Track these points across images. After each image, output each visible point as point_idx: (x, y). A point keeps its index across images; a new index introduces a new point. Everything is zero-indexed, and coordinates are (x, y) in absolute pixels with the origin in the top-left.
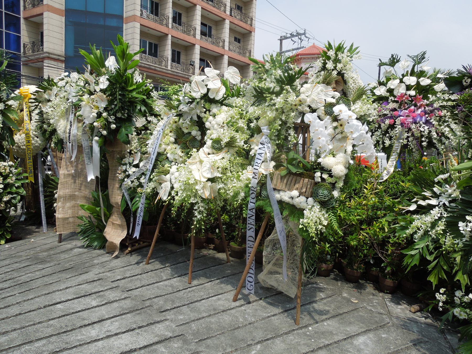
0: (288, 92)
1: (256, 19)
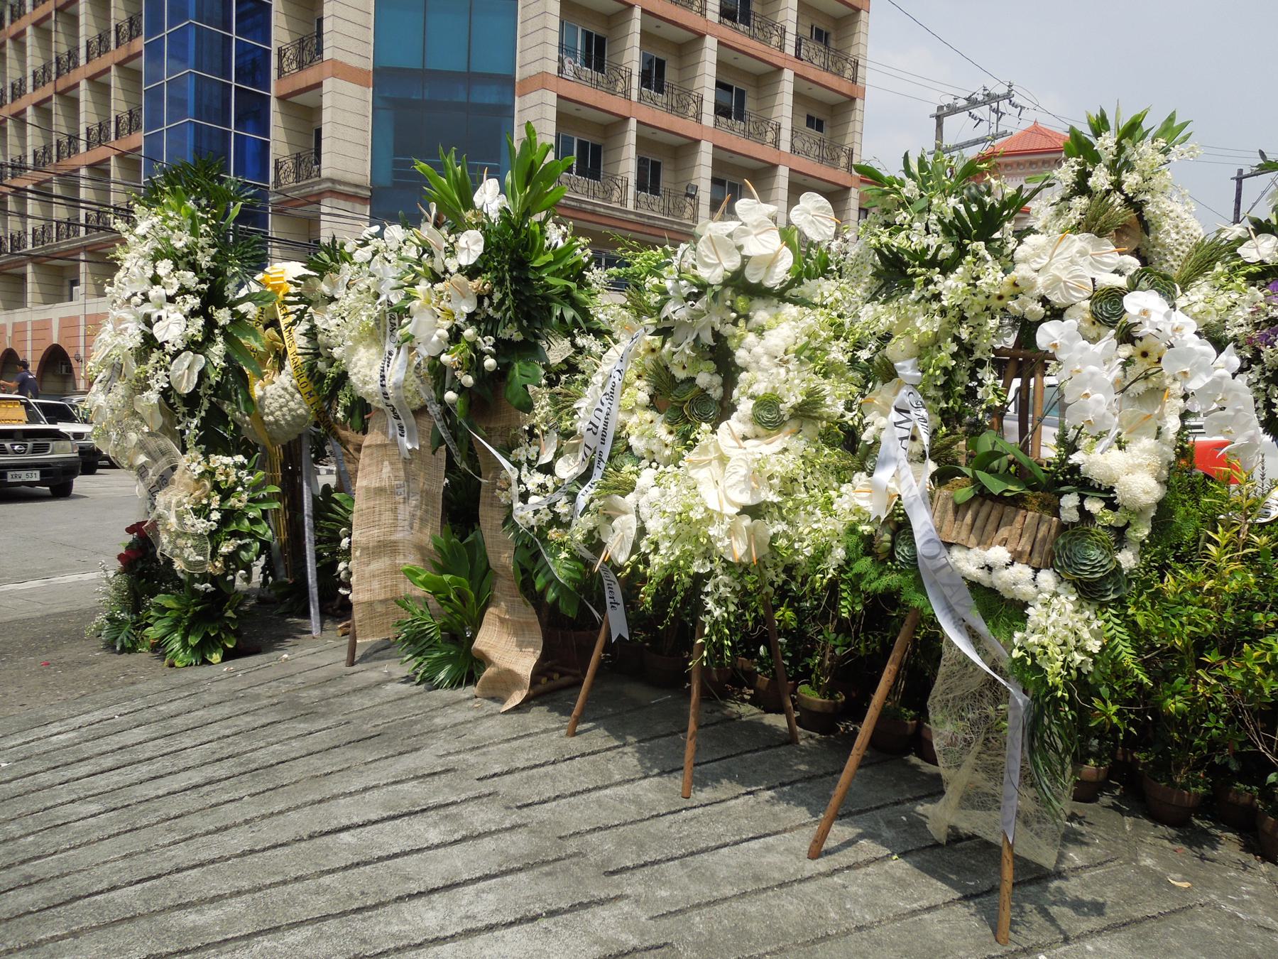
0: (979, 259)
1: (868, 64)
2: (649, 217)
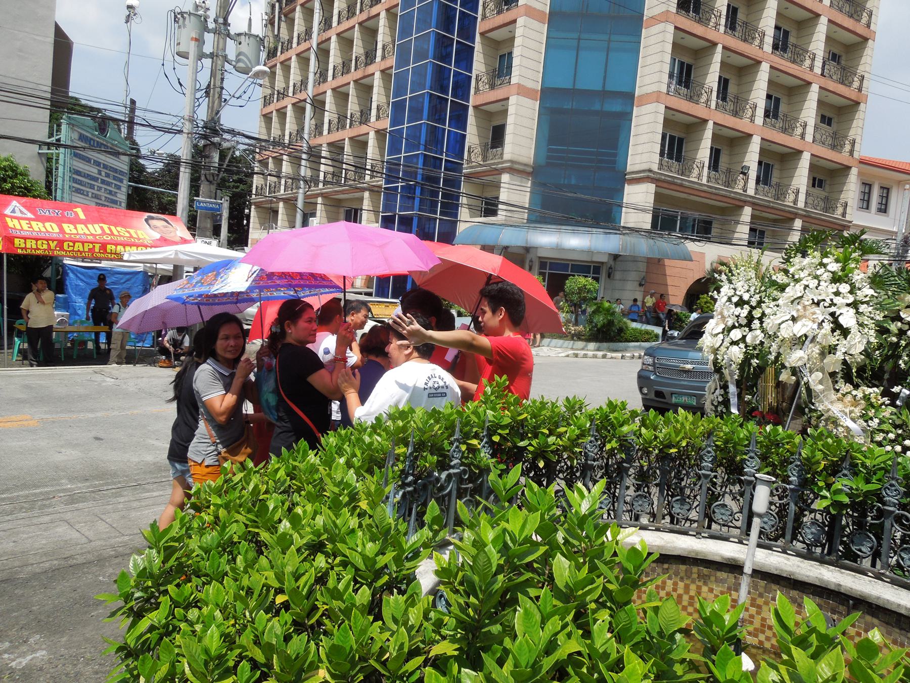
2: (716, 188)
